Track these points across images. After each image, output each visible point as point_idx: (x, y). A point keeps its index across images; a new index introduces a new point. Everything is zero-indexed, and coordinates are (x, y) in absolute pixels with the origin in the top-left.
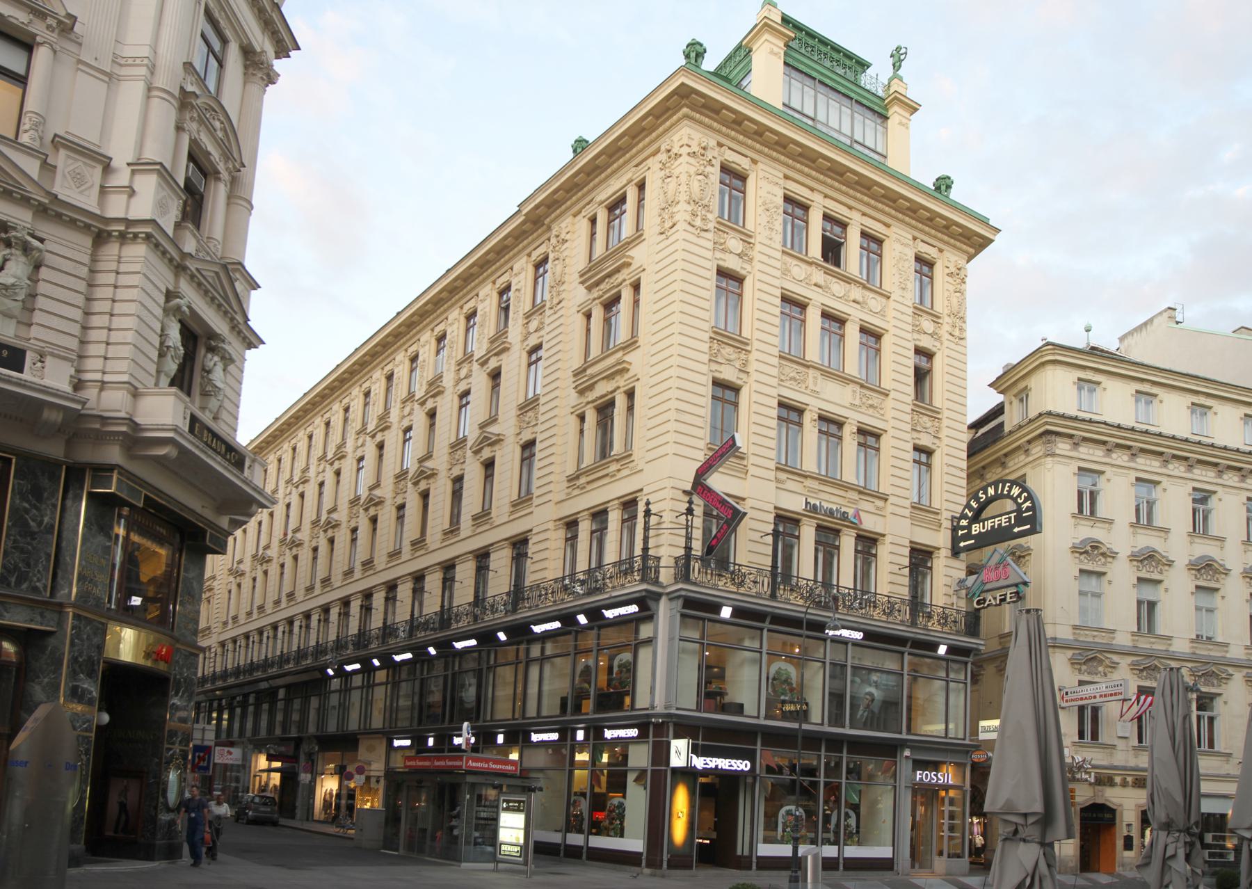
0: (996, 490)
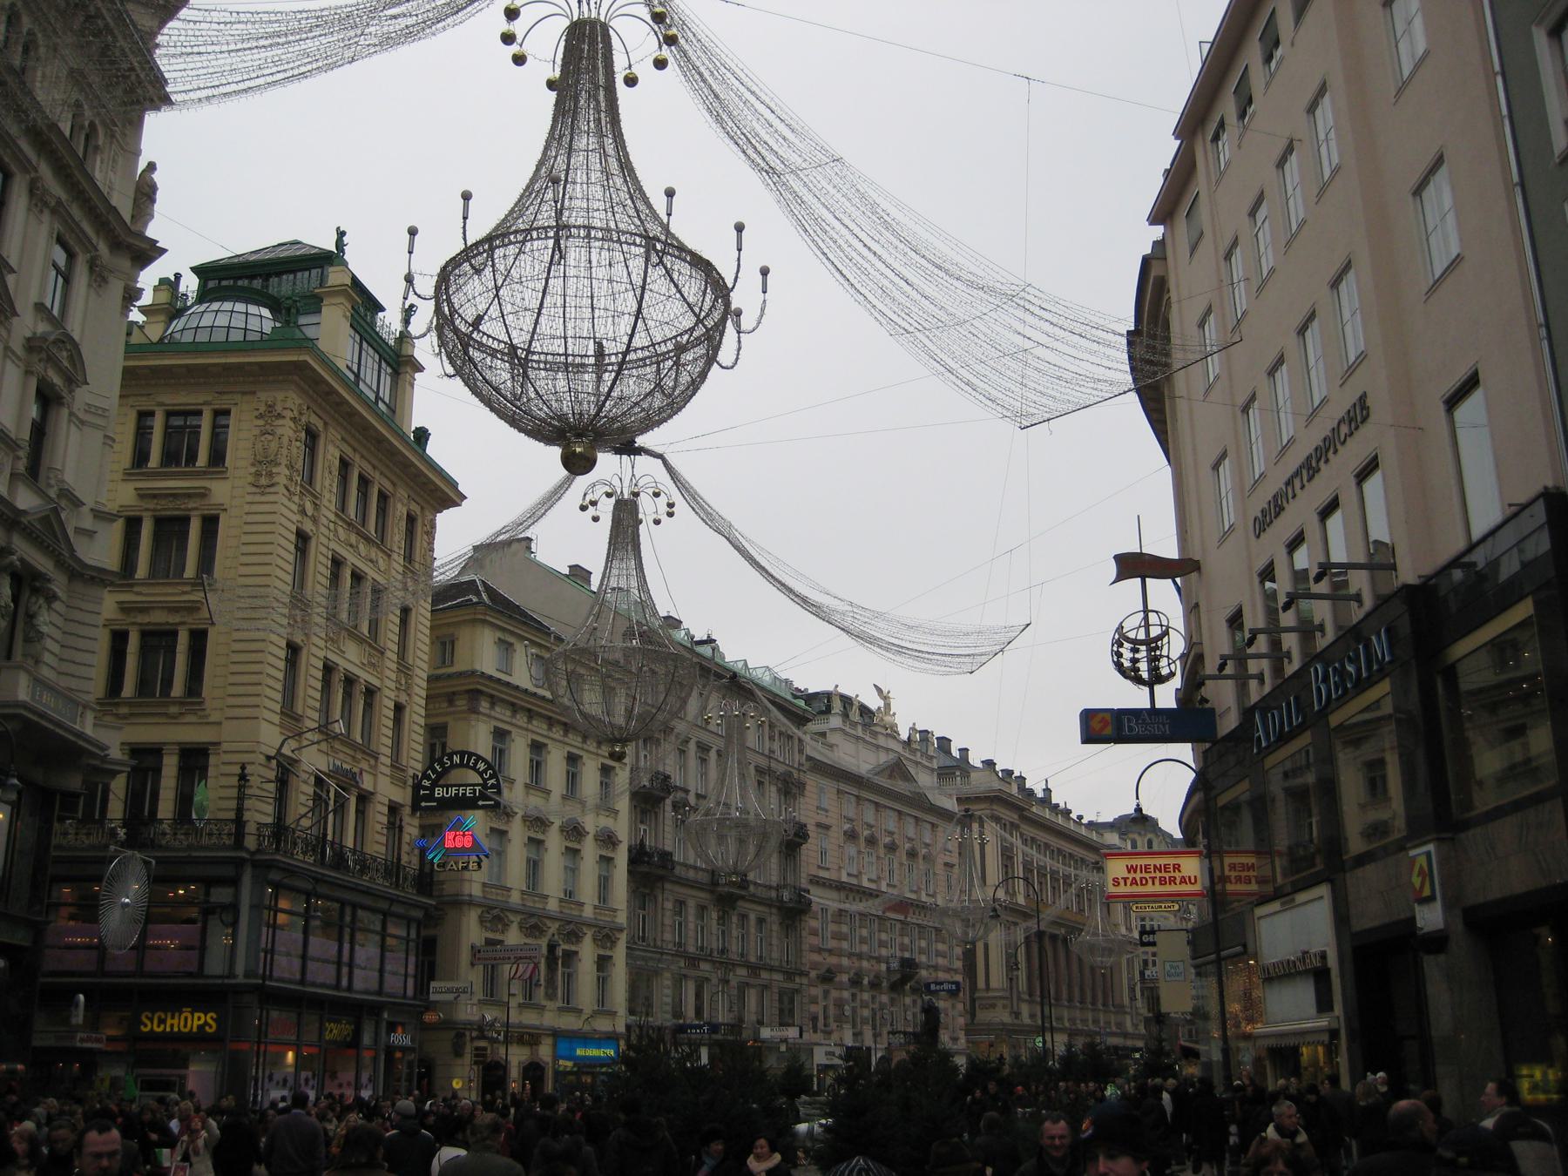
0: (462, 759)
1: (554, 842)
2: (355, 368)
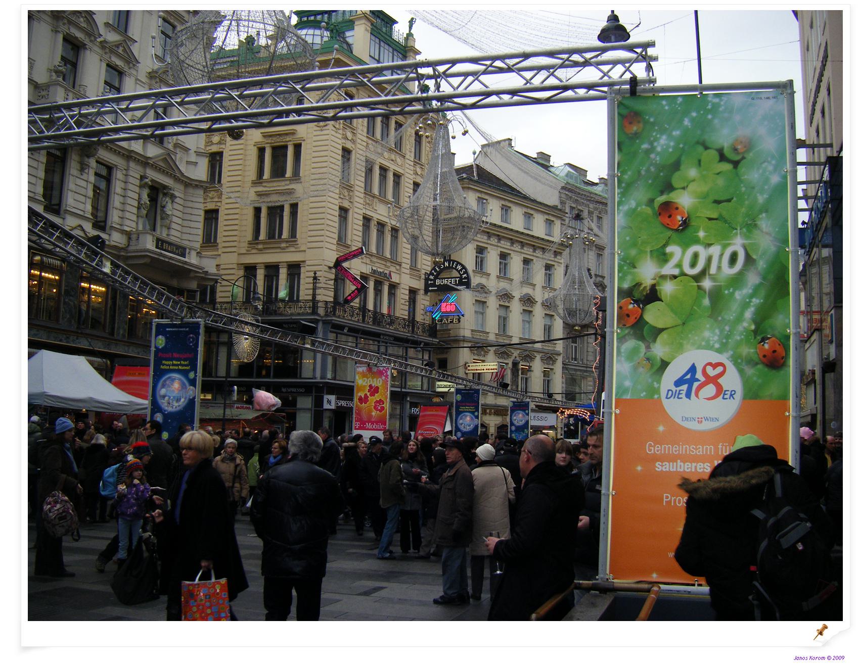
1: (516, 307)
2: (377, 58)
